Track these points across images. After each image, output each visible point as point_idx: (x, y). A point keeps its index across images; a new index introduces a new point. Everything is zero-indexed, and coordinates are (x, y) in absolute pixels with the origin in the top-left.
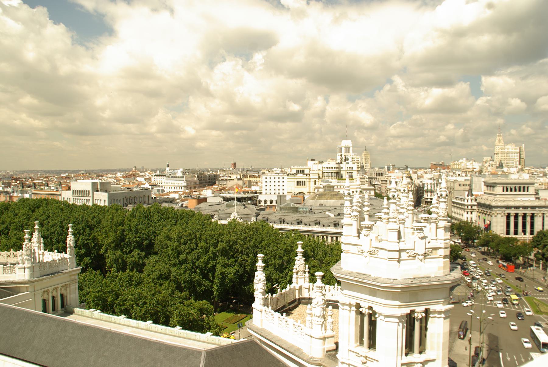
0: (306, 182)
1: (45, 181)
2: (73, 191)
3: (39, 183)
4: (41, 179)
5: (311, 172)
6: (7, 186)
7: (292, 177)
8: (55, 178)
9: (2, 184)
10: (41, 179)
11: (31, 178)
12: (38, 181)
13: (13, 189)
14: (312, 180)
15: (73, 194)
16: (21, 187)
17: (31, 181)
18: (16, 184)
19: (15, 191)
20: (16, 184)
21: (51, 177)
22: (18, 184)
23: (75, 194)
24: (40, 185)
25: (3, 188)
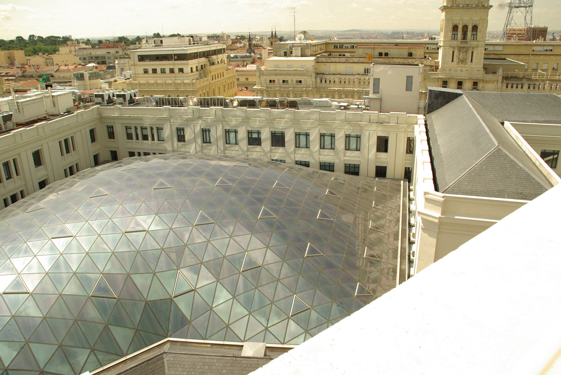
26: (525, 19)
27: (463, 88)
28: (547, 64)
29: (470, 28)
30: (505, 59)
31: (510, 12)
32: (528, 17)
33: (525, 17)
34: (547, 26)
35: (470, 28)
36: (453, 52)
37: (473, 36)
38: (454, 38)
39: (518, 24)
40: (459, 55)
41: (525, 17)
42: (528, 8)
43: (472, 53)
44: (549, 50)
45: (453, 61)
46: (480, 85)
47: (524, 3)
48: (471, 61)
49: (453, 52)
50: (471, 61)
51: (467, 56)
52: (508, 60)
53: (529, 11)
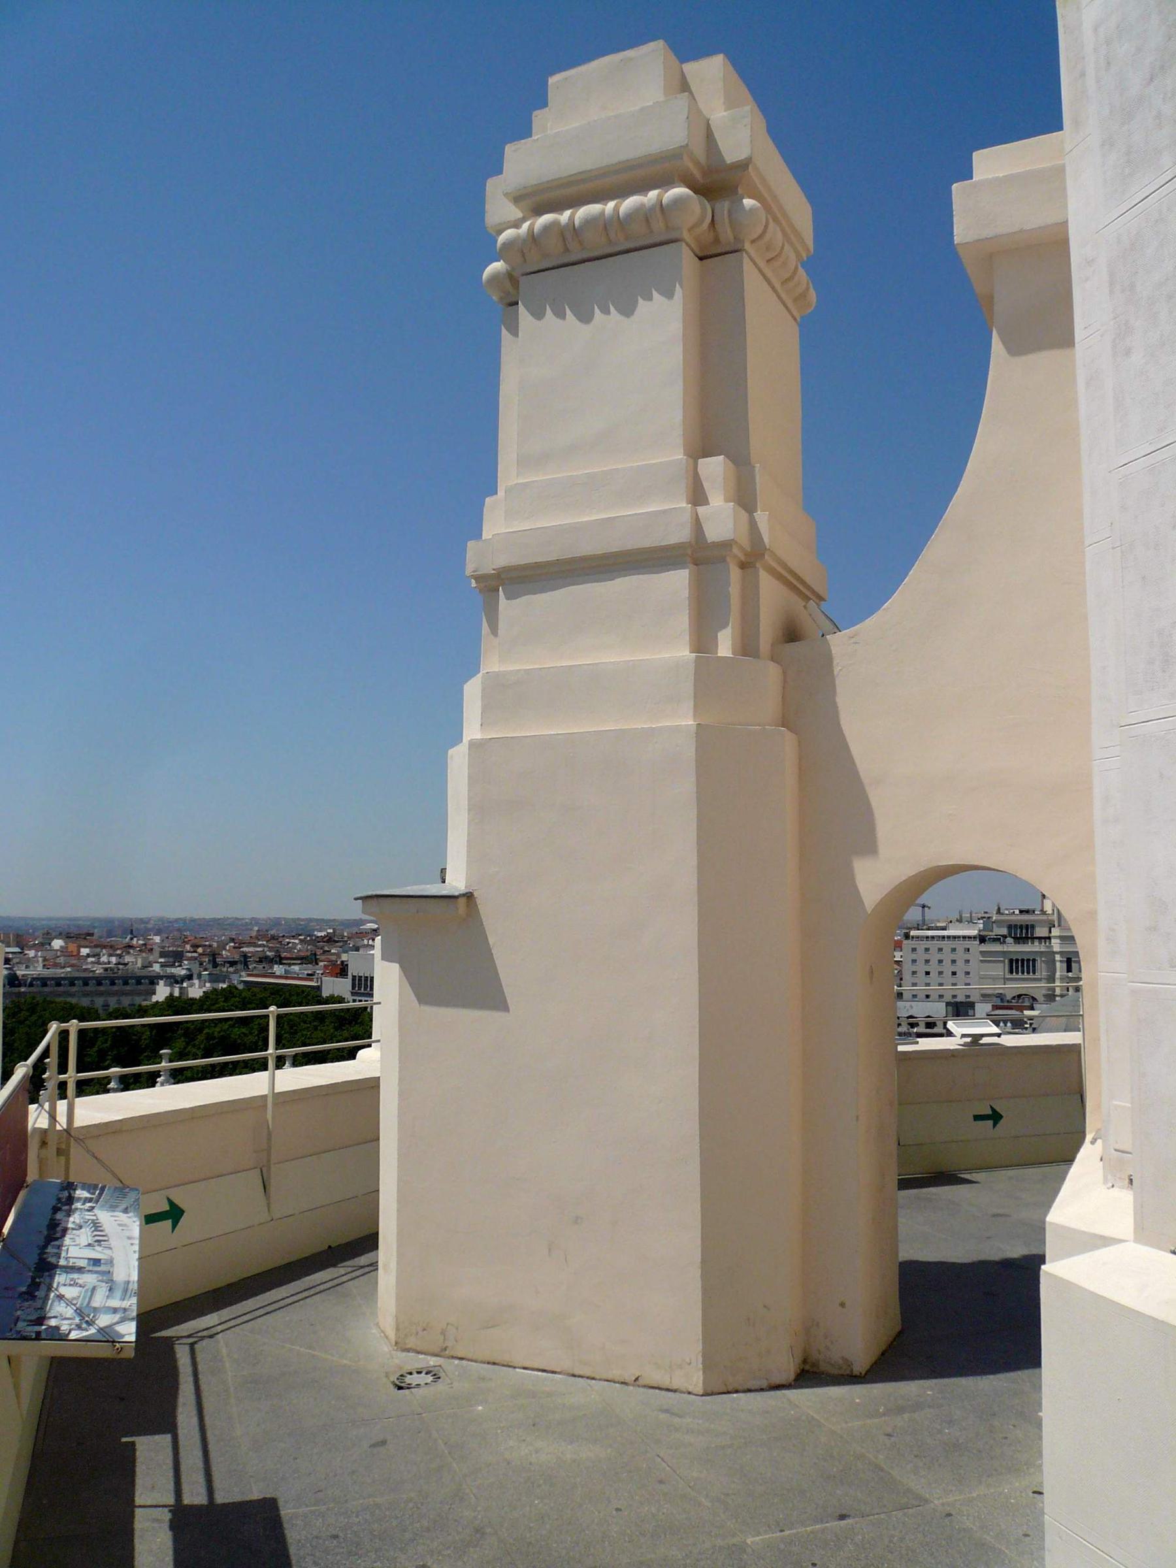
0: (1038, 964)
1: (271, 949)
2: (354, 978)
3: (254, 954)
4: (260, 943)
5: (1055, 932)
6: (171, 960)
7: (997, 947)
8: (297, 941)
9: (161, 957)
10: (260, 943)
11: (232, 940)
12: (251, 949)
13: (188, 969)
14: (1058, 957)
15: (353, 988)
16: (211, 966)
17: (234, 948)
18: (195, 955)
19: (195, 976)
20: (195, 955)
21: (288, 937)
22: (200, 954)
23: (360, 988)
24: (263, 959)
25: (162, 966)
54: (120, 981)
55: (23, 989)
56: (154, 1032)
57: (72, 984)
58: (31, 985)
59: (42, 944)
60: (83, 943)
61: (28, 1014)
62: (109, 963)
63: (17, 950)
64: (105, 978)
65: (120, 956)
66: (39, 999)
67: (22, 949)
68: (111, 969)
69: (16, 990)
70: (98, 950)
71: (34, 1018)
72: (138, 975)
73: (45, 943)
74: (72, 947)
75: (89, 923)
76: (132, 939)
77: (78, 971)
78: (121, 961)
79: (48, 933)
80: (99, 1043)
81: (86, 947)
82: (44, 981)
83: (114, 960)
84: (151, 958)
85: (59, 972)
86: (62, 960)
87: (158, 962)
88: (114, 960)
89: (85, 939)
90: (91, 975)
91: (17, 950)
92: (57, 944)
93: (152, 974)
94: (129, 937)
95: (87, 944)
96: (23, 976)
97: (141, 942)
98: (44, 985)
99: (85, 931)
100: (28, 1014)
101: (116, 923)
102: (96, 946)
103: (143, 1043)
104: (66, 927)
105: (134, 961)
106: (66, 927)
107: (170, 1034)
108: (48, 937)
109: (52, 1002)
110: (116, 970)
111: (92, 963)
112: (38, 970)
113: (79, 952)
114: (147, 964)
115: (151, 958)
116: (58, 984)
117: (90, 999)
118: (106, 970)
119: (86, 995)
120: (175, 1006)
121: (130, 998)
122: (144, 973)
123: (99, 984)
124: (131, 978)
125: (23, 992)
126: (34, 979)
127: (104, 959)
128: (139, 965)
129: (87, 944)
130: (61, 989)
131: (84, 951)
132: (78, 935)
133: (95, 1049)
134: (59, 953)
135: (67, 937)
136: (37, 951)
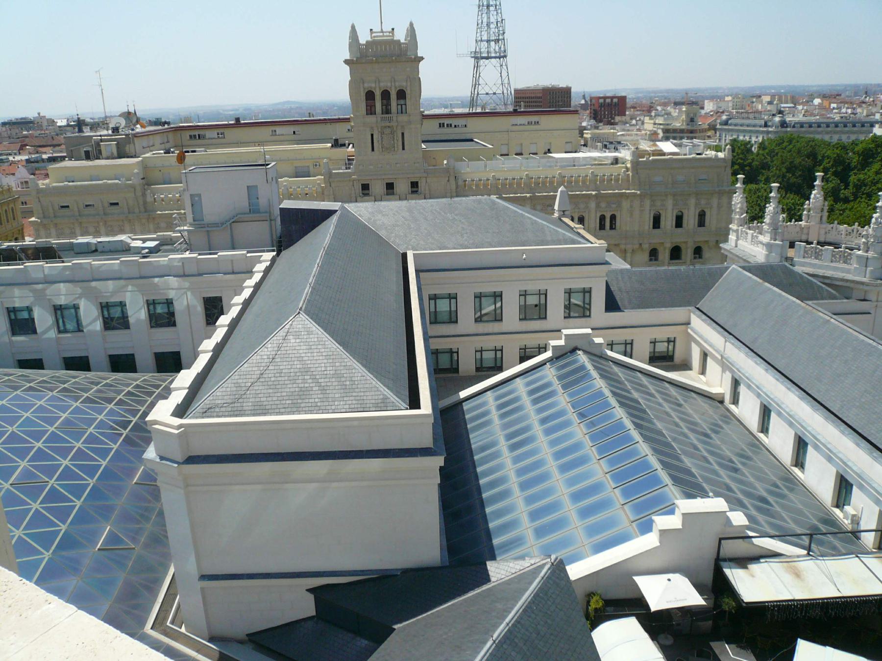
26: (501, 76)
27: (370, 193)
28: (535, 145)
29: (393, 96)
30: (472, 140)
31: (477, 67)
32: (504, 74)
33: (501, 73)
34: (570, 86)
35: (393, 96)
36: (372, 135)
37: (400, 107)
38: (371, 111)
39: (491, 84)
40: (382, 139)
41: (501, 73)
42: (502, 59)
43: (403, 134)
44: (535, 122)
45: (373, 150)
46: (422, 186)
47: (496, 52)
48: (403, 149)
49: (372, 135)
50: (403, 149)
51: (396, 141)
52: (475, 142)
53: (504, 64)
54: (859, 125)
55: (789, 129)
56: (861, 157)
57: (819, 126)
58: (794, 127)
59: (807, 102)
60: (834, 100)
61: (787, 144)
62: (846, 113)
63: (792, 105)
64: (840, 123)
65: (854, 109)
66: (795, 135)
67: (795, 105)
68: (846, 117)
69: (784, 129)
70: (840, 105)
71: (791, 146)
72: (863, 121)
73: (810, 101)
74: (826, 103)
75: (843, 88)
76: (866, 97)
77: (824, 118)
78: (855, 112)
79: (812, 95)
80: (824, 163)
81: (834, 103)
82: (802, 125)
83: (849, 111)
84: (874, 110)
85: (812, 119)
86: (816, 112)
87: (879, 113)
88: (849, 111)
89: (835, 98)
90: (831, 121)
91: (792, 105)
92: (817, 101)
93: (871, 120)
94: (864, 96)
95: (836, 101)
96: (789, 121)
97: (871, 99)
98: (802, 127)
99: (836, 93)
100: (787, 144)
101: (861, 87)
102: (841, 103)
103: (853, 165)
104: (828, 91)
105: (862, 112)
106: (828, 91)
107: (871, 160)
108: (811, 97)
109: (803, 137)
110: (848, 118)
111: (836, 113)
112: (800, 118)
113: (830, 106)
114: (870, 114)
115: (874, 110)
116: (810, 126)
117: (830, 135)
118: (842, 117)
119: (827, 133)
120: (876, 142)
121: (838, 136)
122: (868, 119)
123: (836, 126)
124: (858, 123)
125: (789, 131)
126: (796, 123)
127: (844, 110)
128: (865, 114)
129: (836, 101)
130: (812, 129)
131: (833, 105)
132: (831, 95)
133: (822, 167)
134: (817, 107)
135: (824, 97)
136: (804, 106)
